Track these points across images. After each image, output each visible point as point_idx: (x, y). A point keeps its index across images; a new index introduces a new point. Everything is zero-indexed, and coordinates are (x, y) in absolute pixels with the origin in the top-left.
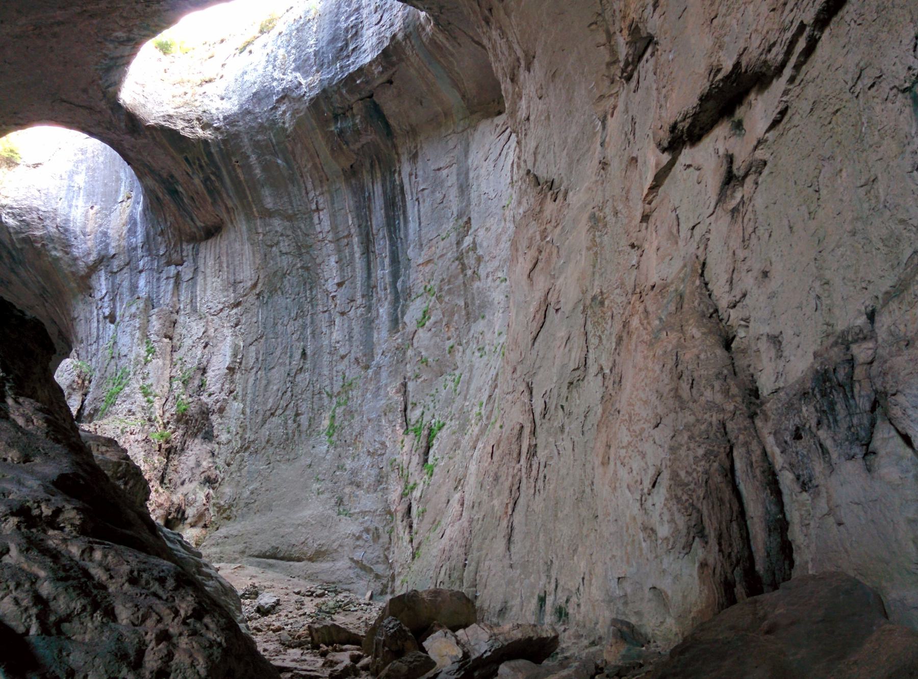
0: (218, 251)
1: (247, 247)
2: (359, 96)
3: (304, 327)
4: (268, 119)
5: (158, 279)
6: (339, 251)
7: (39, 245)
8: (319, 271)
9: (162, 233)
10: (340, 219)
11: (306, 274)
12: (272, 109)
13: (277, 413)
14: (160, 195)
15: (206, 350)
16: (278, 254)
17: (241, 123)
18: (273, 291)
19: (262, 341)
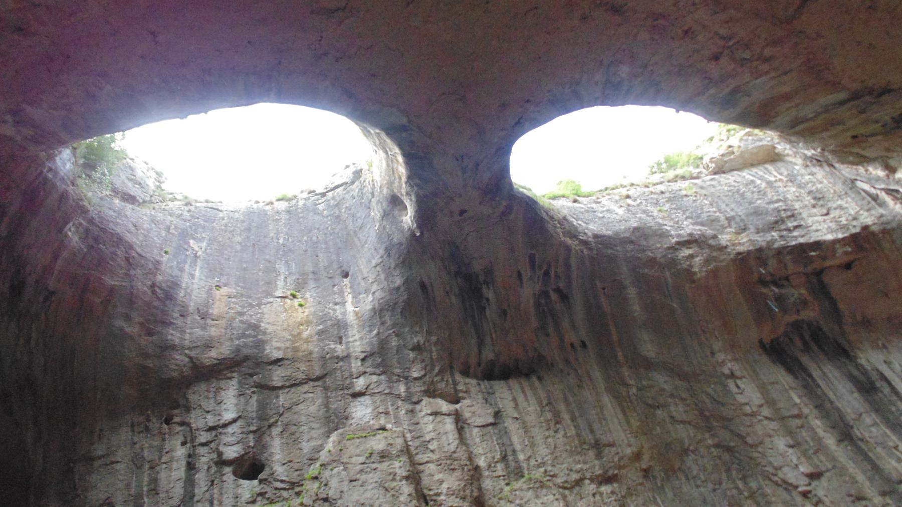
0: (543, 395)
1: (606, 399)
2: (801, 269)
4: (664, 256)
6: (790, 433)
8: (755, 455)
9: (417, 348)
11: (726, 456)
12: (669, 248)
14: (439, 293)
16: (667, 420)
18: (670, 472)
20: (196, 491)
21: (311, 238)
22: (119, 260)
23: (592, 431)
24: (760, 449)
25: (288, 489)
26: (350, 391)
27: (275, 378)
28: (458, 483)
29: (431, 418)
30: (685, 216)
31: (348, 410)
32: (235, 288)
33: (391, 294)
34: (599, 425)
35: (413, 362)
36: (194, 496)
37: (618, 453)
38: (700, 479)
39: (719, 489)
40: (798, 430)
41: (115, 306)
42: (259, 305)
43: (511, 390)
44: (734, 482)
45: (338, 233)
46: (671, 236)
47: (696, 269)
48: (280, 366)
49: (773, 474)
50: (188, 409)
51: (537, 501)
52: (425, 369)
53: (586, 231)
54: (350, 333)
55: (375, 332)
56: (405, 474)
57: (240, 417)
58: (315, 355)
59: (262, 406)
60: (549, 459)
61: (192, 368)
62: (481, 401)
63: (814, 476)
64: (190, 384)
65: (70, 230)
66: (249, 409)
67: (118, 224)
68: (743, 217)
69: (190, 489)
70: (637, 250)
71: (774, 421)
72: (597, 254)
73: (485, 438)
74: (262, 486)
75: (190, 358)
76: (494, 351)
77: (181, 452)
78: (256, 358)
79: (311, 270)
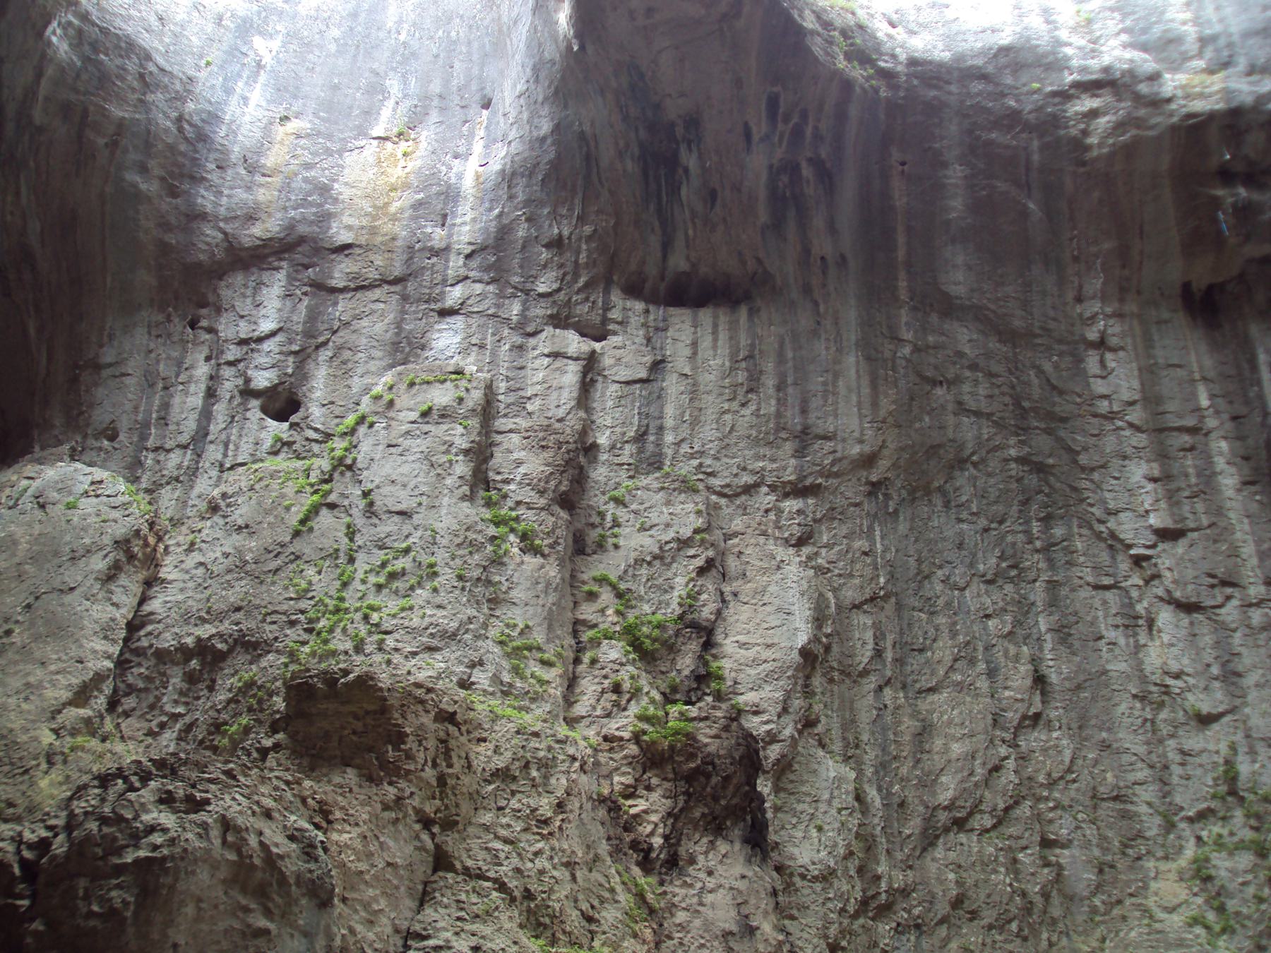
0: (744, 341)
1: (851, 360)
3: (1024, 608)
4: (1039, 109)
6: (1163, 456)
7: (101, 141)
9: (557, 244)
10: (1168, 384)
11: (1032, 480)
12: (1054, 94)
13: (976, 823)
16: (950, 407)
17: (953, 88)
18: (919, 491)
19: (890, 606)
20: (212, 427)
21: (449, 33)
22: (129, 78)
23: (804, 411)
24: (1096, 476)
25: (321, 442)
26: (438, 306)
27: (336, 275)
28: (542, 468)
29: (546, 361)
30: (1121, 26)
31: (428, 334)
32: (310, 121)
33: (532, 149)
34: (821, 403)
35: (545, 266)
36: (207, 434)
37: (835, 452)
38: (969, 508)
39: (995, 529)
40: (1182, 454)
41: (126, 151)
42: (340, 153)
43: (696, 327)
44: (1027, 522)
45: (487, 28)
46: (1068, 68)
47: (1093, 140)
48: (347, 256)
49: (1100, 521)
50: (219, 310)
51: (665, 510)
52: (562, 280)
53: (898, 51)
54: (460, 210)
55: (496, 211)
56: (465, 446)
57: (280, 329)
58: (399, 243)
59: (313, 316)
60: (713, 448)
61: (226, 250)
62: (640, 340)
63: (1166, 535)
64: (224, 274)
65: (54, 33)
66: (295, 318)
67: (130, 17)
68: (1236, 38)
69: (205, 423)
70: (989, 94)
71: (1143, 432)
72: (904, 98)
73: (623, 402)
74: (292, 432)
75: (225, 234)
76: (688, 258)
77: (203, 370)
78: (315, 240)
79: (438, 91)
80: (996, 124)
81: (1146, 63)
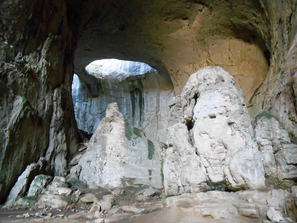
5: (81, 105)
6: (127, 107)
9: (83, 95)
15: (93, 122)
80: (112, 80)
81: (124, 72)
